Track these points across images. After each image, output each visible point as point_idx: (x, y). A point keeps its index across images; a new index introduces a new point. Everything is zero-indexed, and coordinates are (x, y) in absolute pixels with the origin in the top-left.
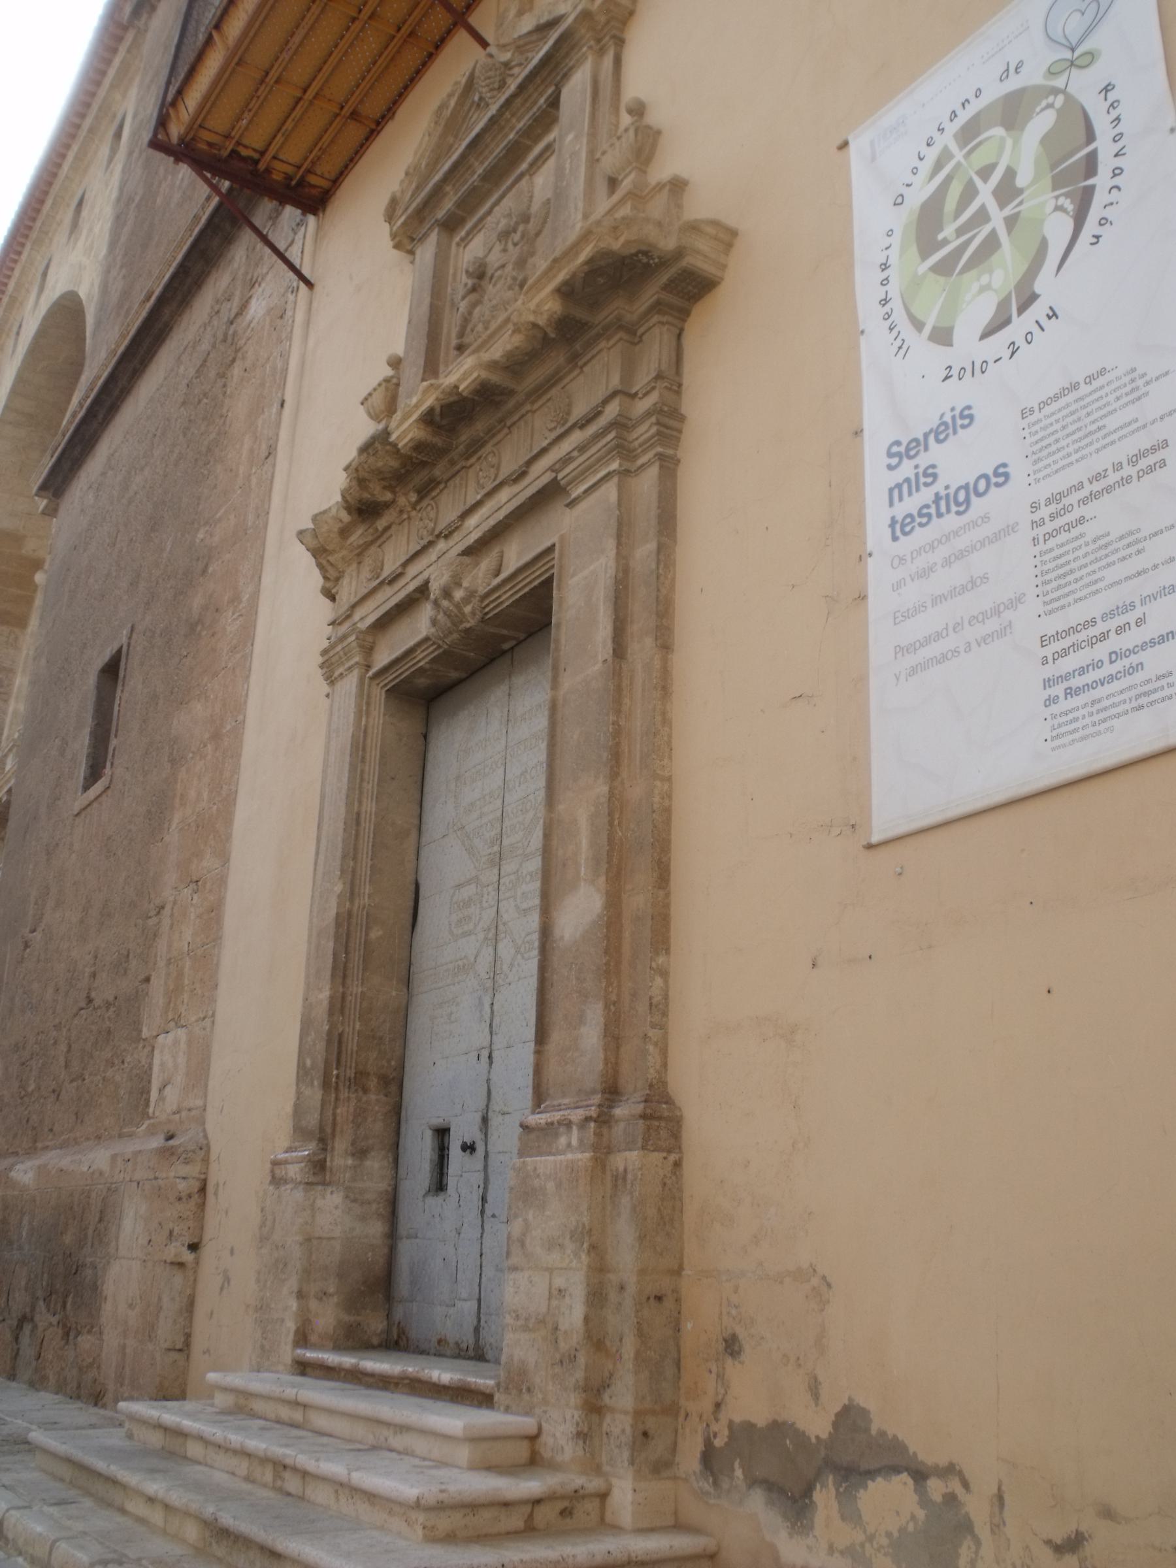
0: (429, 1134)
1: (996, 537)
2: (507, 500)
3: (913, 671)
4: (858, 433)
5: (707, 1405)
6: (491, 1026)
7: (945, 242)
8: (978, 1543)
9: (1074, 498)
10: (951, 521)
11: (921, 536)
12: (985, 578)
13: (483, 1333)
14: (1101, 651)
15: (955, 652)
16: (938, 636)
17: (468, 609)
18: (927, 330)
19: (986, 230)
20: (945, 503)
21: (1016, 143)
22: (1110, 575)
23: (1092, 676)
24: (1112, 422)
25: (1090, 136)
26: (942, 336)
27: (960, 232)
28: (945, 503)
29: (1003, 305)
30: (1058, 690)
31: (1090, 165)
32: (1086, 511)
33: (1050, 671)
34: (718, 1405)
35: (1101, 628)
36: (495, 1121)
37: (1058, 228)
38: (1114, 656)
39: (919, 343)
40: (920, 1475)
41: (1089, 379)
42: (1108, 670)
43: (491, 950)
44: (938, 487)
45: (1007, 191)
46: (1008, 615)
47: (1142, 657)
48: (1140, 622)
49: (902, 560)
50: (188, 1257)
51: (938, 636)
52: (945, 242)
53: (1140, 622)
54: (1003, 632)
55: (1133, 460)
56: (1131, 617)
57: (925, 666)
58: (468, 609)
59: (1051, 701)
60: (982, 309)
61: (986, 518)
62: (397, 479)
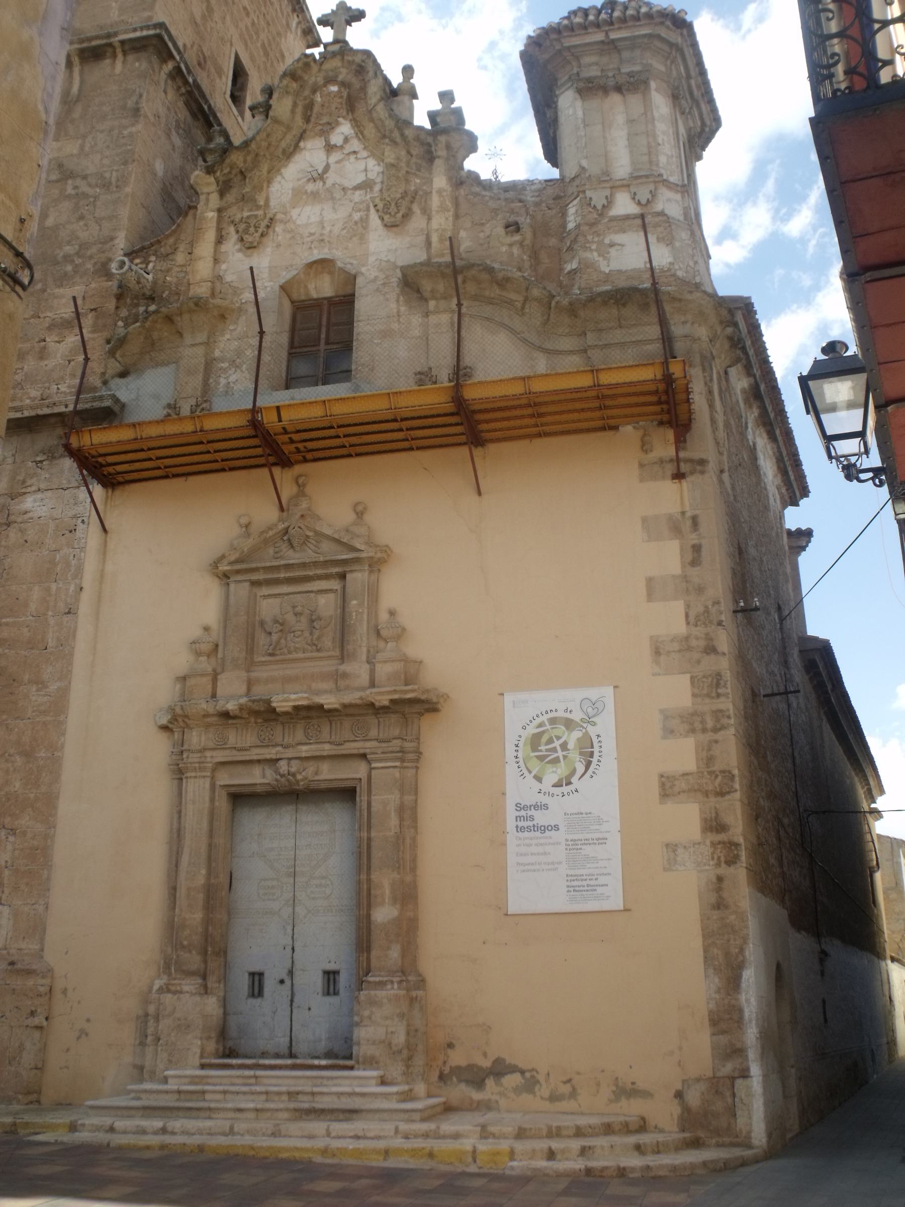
0: (247, 975)
1: (554, 844)
2: (327, 749)
3: (524, 871)
4: (504, 794)
5: (440, 1063)
6: (293, 937)
7: (541, 751)
8: (541, 1085)
9: (579, 842)
10: (538, 834)
11: (526, 834)
12: (549, 854)
13: (293, 1049)
14: (585, 883)
15: (538, 870)
16: (533, 864)
17: (302, 783)
18: (533, 774)
19: (555, 755)
20: (536, 828)
21: (569, 735)
22: (588, 866)
23: (581, 888)
24: (592, 827)
25: (592, 747)
26: (539, 779)
27: (547, 750)
28: (536, 828)
29: (560, 780)
30: (572, 889)
31: (592, 754)
32: (584, 847)
33: (569, 883)
34: (445, 1062)
35: (584, 877)
36: (297, 973)
37: (580, 768)
38: (588, 886)
39: (530, 778)
40: (522, 1072)
41: (587, 814)
42: (586, 888)
43: (291, 909)
44: (535, 822)
45: (564, 746)
46: (556, 866)
47: (597, 888)
48: (596, 879)
49: (520, 839)
50: (45, 1023)
51: (533, 864)
52: (541, 751)
53: (596, 879)
54: (555, 869)
55: (598, 839)
56: (594, 878)
57: (529, 871)
58: (302, 783)
59: (568, 891)
60: (555, 779)
61: (550, 838)
62: (256, 713)
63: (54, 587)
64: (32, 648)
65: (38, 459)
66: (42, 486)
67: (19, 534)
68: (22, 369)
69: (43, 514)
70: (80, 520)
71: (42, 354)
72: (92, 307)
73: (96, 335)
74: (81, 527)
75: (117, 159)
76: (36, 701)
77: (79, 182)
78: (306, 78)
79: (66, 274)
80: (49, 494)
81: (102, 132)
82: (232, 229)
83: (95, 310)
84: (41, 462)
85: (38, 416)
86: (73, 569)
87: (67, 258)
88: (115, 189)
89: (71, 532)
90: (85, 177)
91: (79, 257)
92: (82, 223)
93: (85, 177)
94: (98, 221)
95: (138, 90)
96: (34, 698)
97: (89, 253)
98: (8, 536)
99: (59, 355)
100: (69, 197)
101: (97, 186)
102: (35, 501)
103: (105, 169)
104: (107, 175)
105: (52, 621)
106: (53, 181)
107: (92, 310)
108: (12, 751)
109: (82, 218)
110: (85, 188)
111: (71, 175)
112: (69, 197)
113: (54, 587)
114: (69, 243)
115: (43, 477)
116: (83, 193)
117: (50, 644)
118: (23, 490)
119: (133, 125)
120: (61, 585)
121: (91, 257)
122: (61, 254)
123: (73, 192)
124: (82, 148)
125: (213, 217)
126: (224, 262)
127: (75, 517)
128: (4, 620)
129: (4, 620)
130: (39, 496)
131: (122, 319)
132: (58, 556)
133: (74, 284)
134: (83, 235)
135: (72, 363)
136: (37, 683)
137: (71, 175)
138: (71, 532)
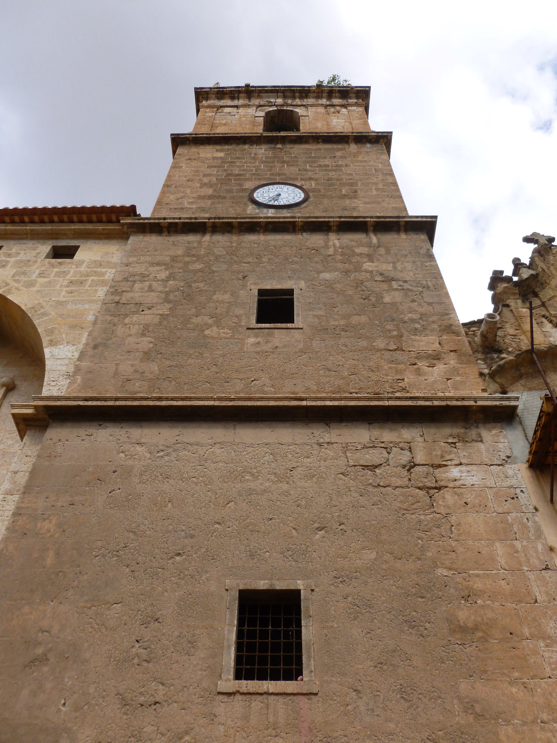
63: (518, 544)
64: (520, 601)
65: (450, 441)
66: (463, 461)
67: (456, 497)
68: (403, 380)
69: (476, 483)
70: (518, 491)
71: (418, 372)
72: (452, 349)
73: (464, 366)
74: (520, 495)
75: (428, 276)
76: (551, 657)
77: (401, 283)
78: (547, 257)
79: (416, 329)
80: (474, 468)
81: (407, 262)
82: (544, 320)
83: (455, 351)
84: (455, 443)
85: (448, 406)
86: (532, 531)
87: (413, 321)
88: (434, 290)
89: (513, 498)
90: (405, 282)
91: (423, 321)
92: (416, 304)
93: (405, 282)
94: (430, 304)
95: (424, 247)
96: (546, 655)
97: (431, 319)
98: (444, 498)
99: (435, 375)
100: (396, 289)
101: (418, 287)
102: (461, 472)
103: (419, 279)
104: (424, 282)
105: (531, 576)
106: (380, 281)
107: (451, 351)
108: (545, 717)
109: (413, 301)
110: (406, 286)
111: (393, 279)
112: (396, 289)
113: (518, 544)
114: (410, 313)
115: (461, 455)
116: (408, 289)
117: (539, 599)
118: (444, 463)
119: (431, 261)
120: (525, 543)
121: (433, 322)
122: (406, 318)
123: (399, 288)
124: (395, 268)
125: (526, 312)
126: (551, 337)
127: (511, 487)
128: (471, 572)
129: (471, 572)
130: (463, 468)
131: (480, 359)
132: (509, 518)
133: (427, 335)
134: (423, 310)
135: (450, 381)
136: (544, 639)
137: (393, 279)
138: (513, 498)
